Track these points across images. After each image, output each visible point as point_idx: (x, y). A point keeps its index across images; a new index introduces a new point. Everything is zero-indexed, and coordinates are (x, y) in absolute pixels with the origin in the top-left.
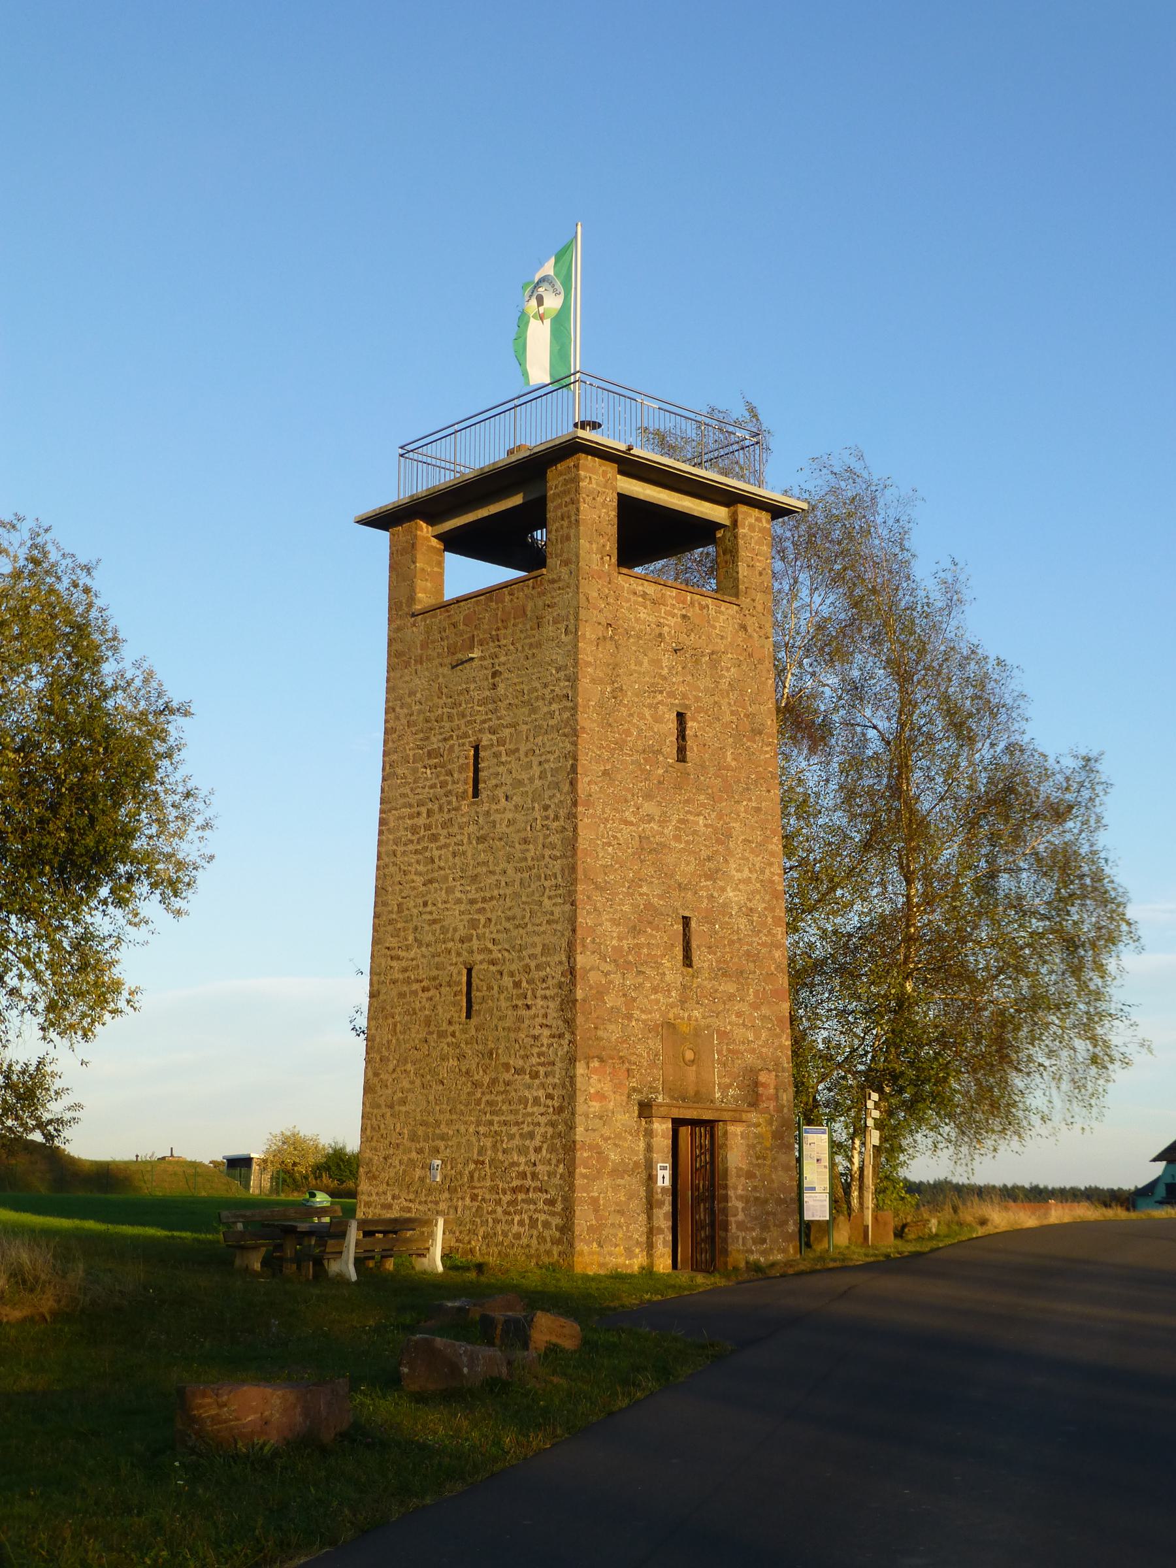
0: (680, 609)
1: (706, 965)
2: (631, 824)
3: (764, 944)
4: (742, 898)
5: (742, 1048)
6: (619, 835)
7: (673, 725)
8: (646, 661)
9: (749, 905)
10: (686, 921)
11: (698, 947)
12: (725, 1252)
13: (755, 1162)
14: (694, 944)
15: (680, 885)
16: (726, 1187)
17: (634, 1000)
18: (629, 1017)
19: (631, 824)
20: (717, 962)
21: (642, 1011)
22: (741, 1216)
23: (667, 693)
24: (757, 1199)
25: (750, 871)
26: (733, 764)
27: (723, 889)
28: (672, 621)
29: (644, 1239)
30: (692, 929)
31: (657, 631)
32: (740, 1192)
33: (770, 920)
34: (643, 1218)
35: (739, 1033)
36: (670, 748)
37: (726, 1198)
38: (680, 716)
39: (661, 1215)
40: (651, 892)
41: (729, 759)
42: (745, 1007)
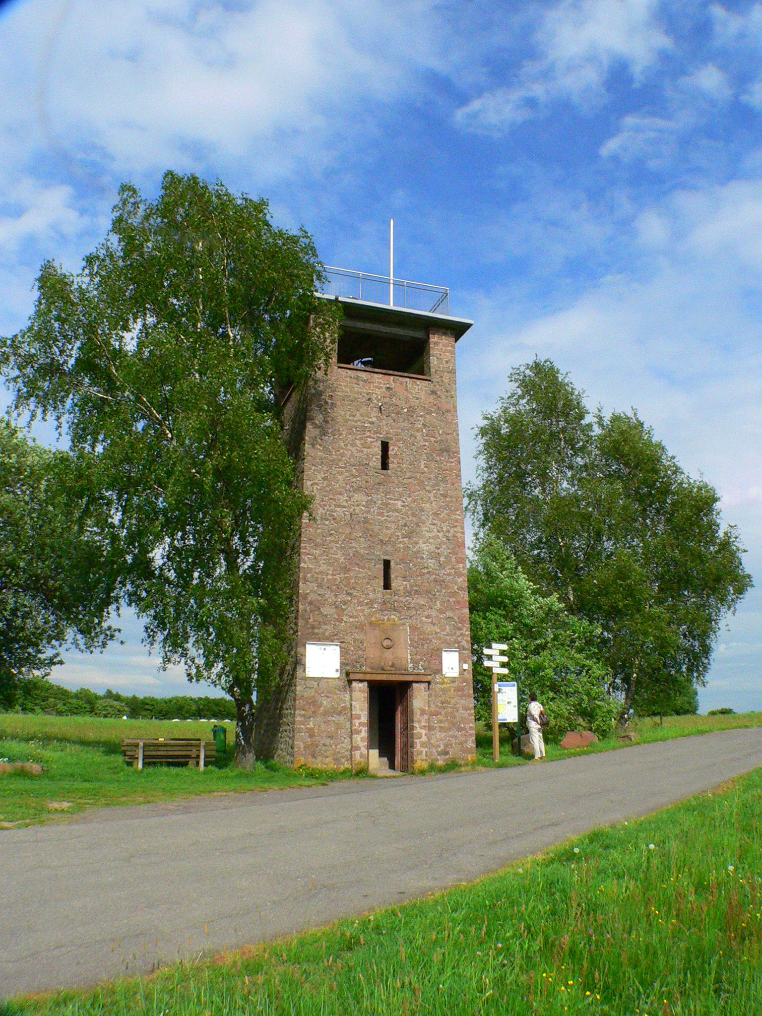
0: (384, 384)
1: (402, 588)
2: (344, 507)
3: (449, 575)
4: (432, 548)
5: (430, 637)
6: (335, 514)
7: (378, 450)
8: (358, 414)
9: (437, 551)
10: (387, 564)
11: (396, 577)
12: (413, 762)
13: (440, 705)
14: (393, 576)
15: (382, 541)
16: (412, 721)
17: (344, 610)
18: (341, 621)
19: (344, 507)
20: (410, 585)
21: (351, 617)
22: (424, 739)
23: (374, 431)
24: (441, 728)
25: (438, 531)
26: (426, 469)
27: (417, 543)
28: (378, 391)
29: (348, 753)
30: (392, 567)
31: (368, 397)
32: (423, 724)
33: (454, 560)
34: (347, 740)
35: (429, 628)
36: (376, 462)
37: (413, 728)
38: (385, 447)
39: (359, 739)
40: (361, 546)
41: (422, 466)
42: (434, 613)
